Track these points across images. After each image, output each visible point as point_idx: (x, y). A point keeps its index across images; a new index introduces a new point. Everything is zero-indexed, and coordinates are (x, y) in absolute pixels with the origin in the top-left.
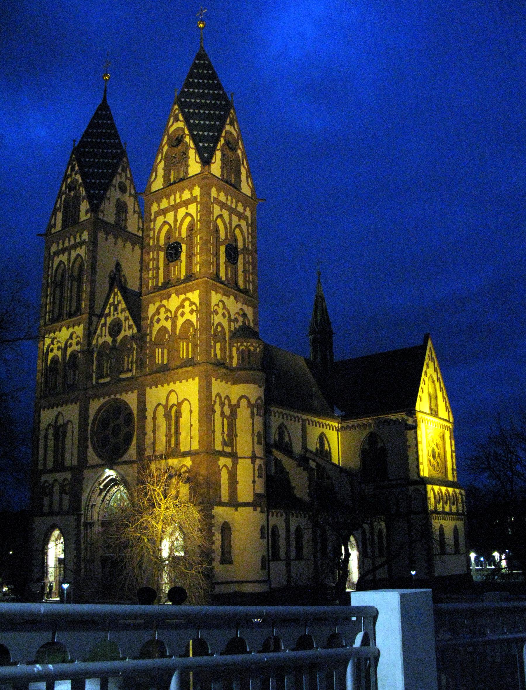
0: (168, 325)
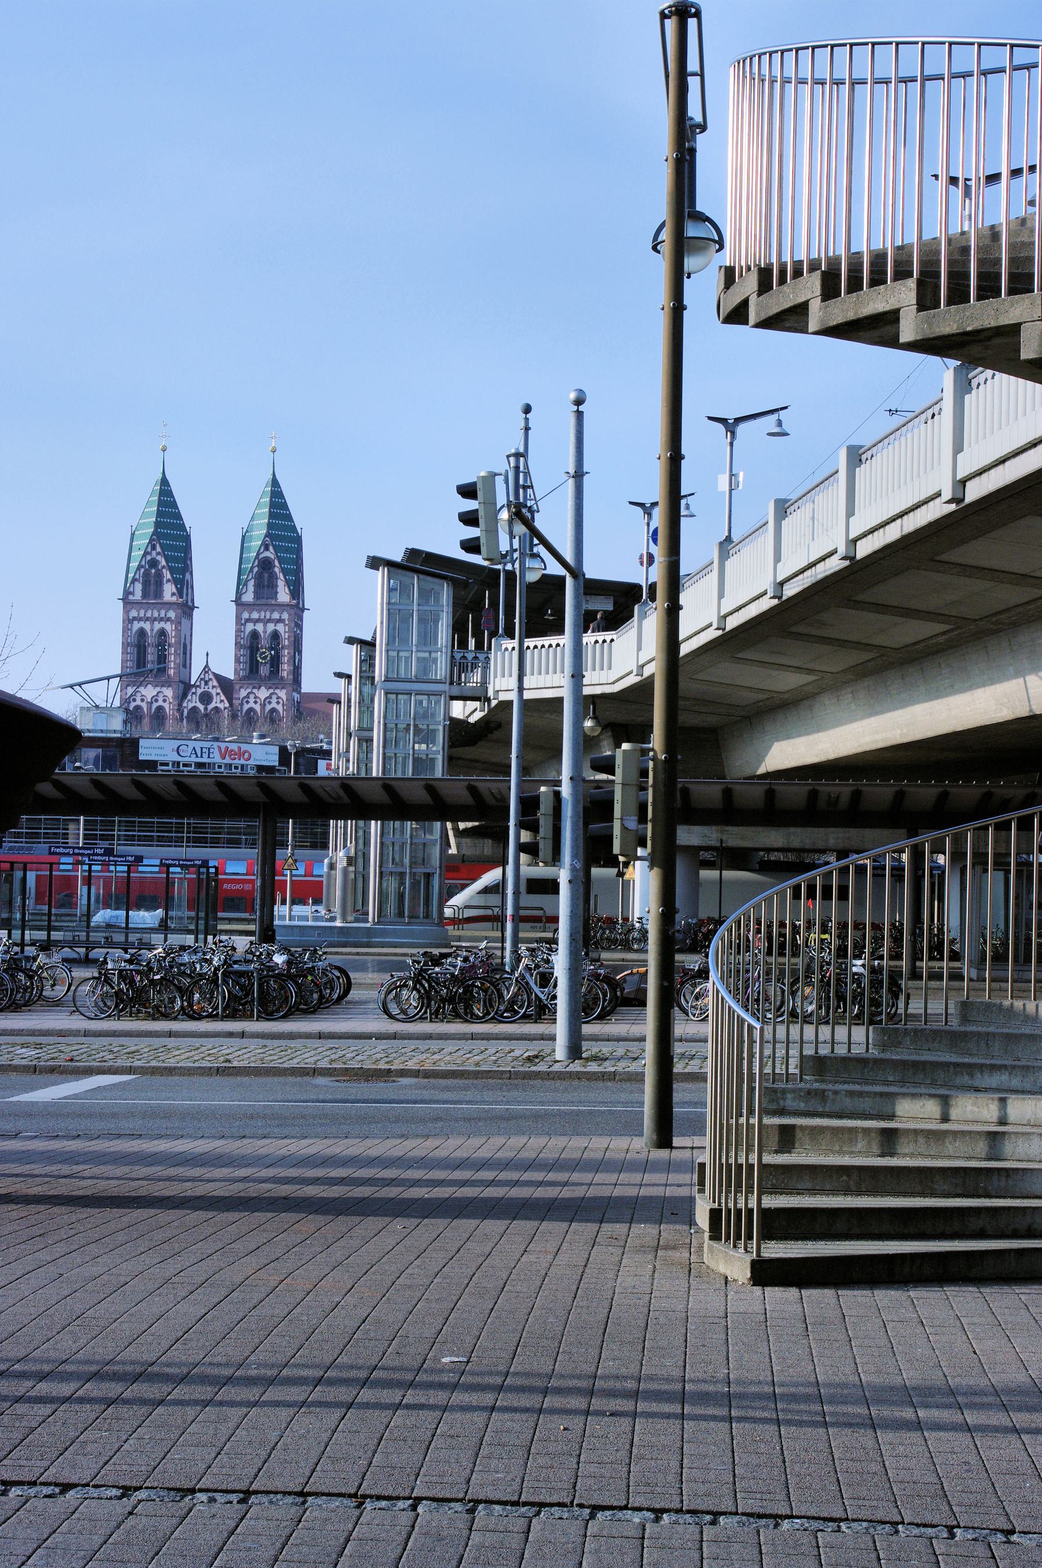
0: (257, 708)
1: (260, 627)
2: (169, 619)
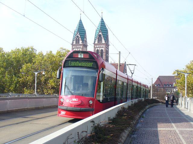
1: (99, 49)
2: (81, 48)
